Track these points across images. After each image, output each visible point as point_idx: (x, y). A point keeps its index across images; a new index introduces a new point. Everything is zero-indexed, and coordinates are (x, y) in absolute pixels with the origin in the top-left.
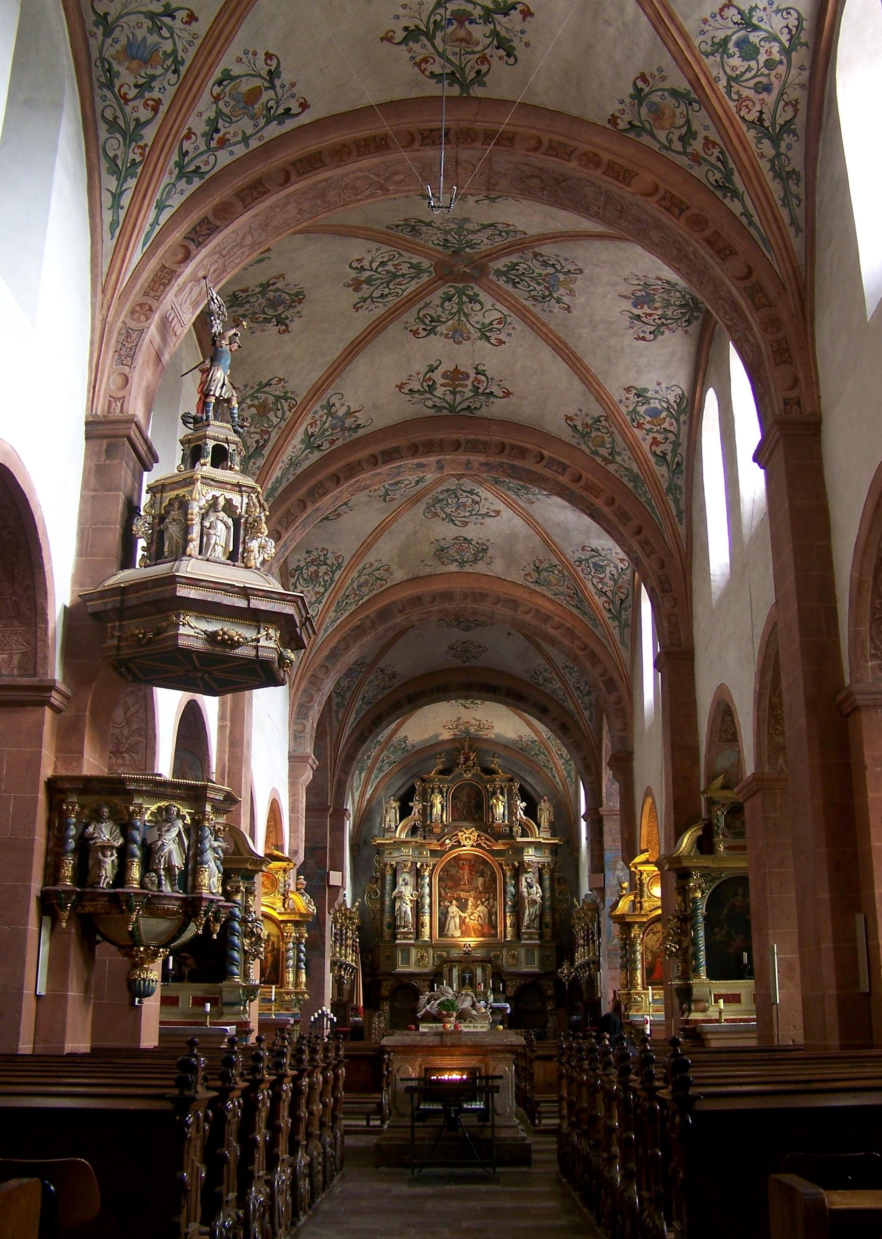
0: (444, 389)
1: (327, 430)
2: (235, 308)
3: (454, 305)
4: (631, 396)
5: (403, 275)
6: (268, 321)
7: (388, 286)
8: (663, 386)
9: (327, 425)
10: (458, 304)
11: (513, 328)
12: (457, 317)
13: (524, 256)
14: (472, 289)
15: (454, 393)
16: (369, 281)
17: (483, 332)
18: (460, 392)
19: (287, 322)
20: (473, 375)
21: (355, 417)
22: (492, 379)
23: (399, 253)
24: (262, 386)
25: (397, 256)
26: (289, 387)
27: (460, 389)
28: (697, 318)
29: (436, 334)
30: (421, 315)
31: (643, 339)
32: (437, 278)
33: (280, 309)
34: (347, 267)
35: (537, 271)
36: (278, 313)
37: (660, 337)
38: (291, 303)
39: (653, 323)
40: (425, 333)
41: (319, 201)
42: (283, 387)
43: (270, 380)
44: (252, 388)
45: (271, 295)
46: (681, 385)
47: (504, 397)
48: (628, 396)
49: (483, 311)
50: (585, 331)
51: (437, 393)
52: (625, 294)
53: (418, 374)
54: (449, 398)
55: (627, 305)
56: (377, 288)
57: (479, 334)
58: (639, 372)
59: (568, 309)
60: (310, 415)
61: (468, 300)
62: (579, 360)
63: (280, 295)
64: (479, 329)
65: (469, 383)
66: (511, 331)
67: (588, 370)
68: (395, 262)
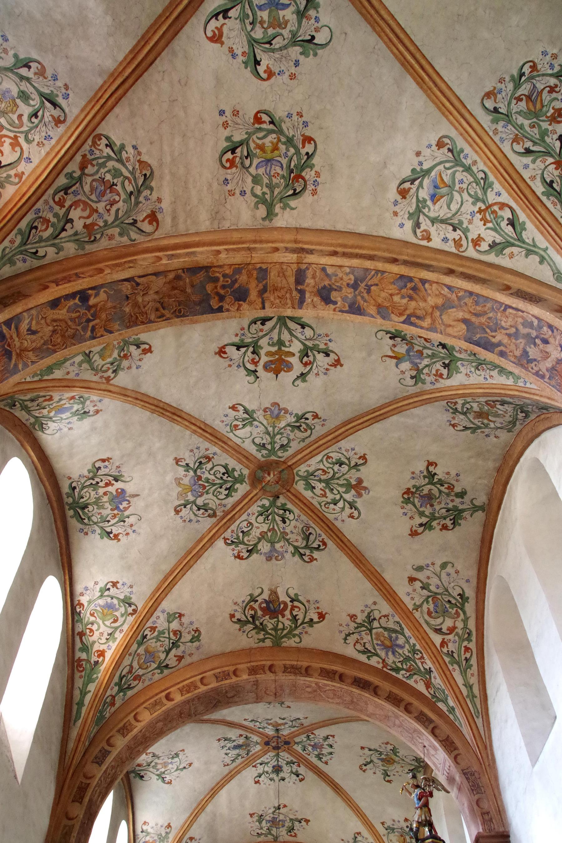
0: (291, 350)
1: (428, 356)
2: (461, 507)
3: (278, 441)
4: (92, 409)
5: (320, 481)
6: (441, 483)
7: (334, 474)
8: (65, 430)
9: (426, 362)
10: (275, 443)
11: (223, 422)
12: (276, 430)
13: (223, 508)
14: (262, 455)
15: (280, 343)
16: (349, 486)
17: (252, 417)
18: (273, 345)
19: (425, 473)
20: (260, 368)
21: (393, 351)
22: (239, 366)
23: (321, 506)
24: (474, 430)
25: (323, 504)
26: (448, 416)
27: (274, 349)
28: (68, 495)
29: (297, 415)
30: (309, 431)
31: (103, 461)
32: (293, 467)
33: (426, 491)
34: (362, 516)
35: (210, 496)
36: (429, 487)
37: (90, 467)
38: (415, 493)
39: (101, 477)
40: (307, 416)
41: (355, 700)
42: (454, 418)
43: (463, 430)
44: (483, 432)
45: (428, 511)
46: (49, 437)
47: (224, 347)
48: (96, 408)
49: (252, 437)
50: (158, 445)
51: (299, 346)
52: (136, 499)
53: (317, 374)
54: (286, 336)
55: (130, 488)
56: (344, 475)
57: (255, 415)
58: (93, 429)
59: (177, 461)
60: (438, 385)
61: (266, 446)
62: (153, 411)
63: (421, 506)
64: (255, 420)
65: (264, 359)
66: (225, 419)
67: (143, 407)
68: (324, 499)
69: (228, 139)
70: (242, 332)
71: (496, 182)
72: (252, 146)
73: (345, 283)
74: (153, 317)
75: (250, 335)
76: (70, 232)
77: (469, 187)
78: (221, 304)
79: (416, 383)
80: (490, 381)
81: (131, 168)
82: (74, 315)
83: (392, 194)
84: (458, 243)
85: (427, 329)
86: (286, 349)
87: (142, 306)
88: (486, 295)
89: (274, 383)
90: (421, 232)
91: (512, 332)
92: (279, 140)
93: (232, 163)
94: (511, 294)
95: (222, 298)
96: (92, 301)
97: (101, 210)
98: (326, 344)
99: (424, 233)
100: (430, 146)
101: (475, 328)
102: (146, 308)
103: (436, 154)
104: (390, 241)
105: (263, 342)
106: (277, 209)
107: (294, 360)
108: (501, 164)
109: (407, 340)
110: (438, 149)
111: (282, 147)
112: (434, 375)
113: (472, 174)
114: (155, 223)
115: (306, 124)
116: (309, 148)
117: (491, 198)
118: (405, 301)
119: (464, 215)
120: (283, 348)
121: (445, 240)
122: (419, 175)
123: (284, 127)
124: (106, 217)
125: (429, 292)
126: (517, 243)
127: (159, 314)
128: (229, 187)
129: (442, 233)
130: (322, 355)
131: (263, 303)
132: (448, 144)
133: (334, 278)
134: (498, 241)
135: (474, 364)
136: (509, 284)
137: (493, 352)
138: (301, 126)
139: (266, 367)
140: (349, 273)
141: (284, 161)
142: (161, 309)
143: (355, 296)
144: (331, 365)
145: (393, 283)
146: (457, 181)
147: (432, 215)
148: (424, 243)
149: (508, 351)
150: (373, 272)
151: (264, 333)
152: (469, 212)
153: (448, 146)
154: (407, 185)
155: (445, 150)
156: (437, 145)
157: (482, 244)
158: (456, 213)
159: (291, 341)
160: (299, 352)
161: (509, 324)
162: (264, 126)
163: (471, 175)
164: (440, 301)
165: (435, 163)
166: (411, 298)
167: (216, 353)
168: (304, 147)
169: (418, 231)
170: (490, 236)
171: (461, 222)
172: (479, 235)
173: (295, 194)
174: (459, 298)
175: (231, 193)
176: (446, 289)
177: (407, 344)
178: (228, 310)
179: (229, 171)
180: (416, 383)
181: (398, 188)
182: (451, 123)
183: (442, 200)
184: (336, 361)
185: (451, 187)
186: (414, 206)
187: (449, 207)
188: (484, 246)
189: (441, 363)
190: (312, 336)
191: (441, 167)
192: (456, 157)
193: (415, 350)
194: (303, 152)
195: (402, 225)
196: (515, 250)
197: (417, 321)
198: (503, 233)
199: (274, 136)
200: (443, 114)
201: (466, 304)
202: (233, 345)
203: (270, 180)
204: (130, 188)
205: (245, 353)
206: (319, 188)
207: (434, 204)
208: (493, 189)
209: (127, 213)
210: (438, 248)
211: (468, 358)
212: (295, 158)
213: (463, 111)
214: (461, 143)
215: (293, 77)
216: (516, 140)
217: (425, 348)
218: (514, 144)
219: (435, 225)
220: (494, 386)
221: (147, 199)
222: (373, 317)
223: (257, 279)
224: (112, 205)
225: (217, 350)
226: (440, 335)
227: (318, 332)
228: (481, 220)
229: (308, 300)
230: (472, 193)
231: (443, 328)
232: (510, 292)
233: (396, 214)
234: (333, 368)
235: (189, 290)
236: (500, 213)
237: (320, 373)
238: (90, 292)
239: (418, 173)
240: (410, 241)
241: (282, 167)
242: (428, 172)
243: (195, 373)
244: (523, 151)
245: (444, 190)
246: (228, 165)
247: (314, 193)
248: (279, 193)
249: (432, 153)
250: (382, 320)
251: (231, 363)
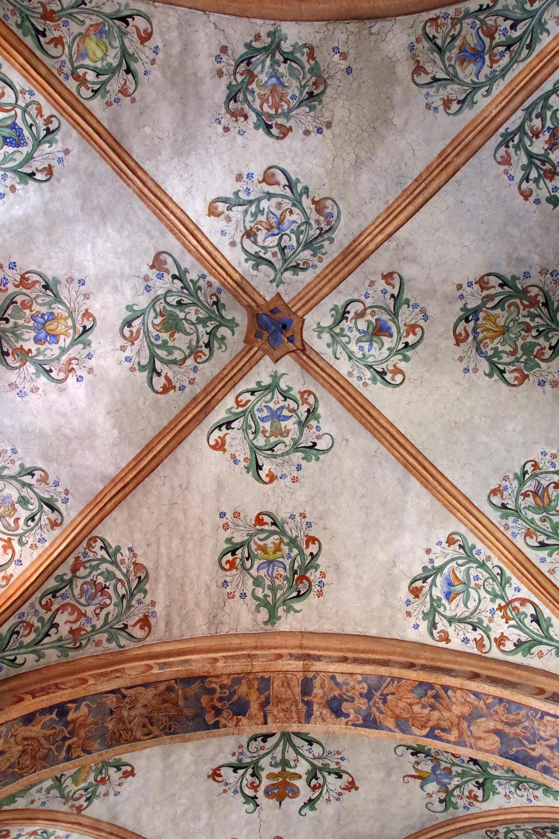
0: (296, 771)
1: (458, 775)
9: (456, 781)
15: (285, 763)
18: (276, 765)
21: (417, 770)
22: (235, 792)
47: (218, 768)
54: (291, 755)
60: (473, 810)
65: (265, 782)
69: (228, 540)
70: (240, 750)
71: (513, 577)
72: (253, 547)
73: (357, 693)
74: (138, 734)
75: (249, 754)
76: (54, 637)
77: (486, 583)
78: (217, 719)
79: (446, 809)
80: (535, 803)
81: (125, 571)
82: (49, 732)
83: (404, 593)
84: (479, 643)
85: (455, 743)
86: (292, 771)
87: (127, 722)
88: (518, 701)
89: (277, 811)
90: (438, 633)
91: (554, 743)
92: (281, 541)
93: (232, 565)
94: (547, 699)
95: (218, 712)
96: (71, 716)
97: (89, 614)
98: (337, 763)
99: (442, 634)
100: (439, 543)
101: (510, 740)
102: (132, 724)
103: (447, 551)
104: (404, 644)
105: (265, 762)
106: (280, 611)
107: (301, 784)
108: (516, 559)
109: (431, 756)
110: (449, 546)
111: (285, 549)
112: (467, 797)
113: (487, 570)
114: (147, 628)
115: (309, 525)
116: (313, 549)
117: (510, 594)
118: (426, 711)
119: (484, 613)
120: (288, 769)
121: (466, 640)
122: (430, 573)
123: (287, 528)
124: (94, 622)
125: (454, 700)
126: (544, 640)
127: (145, 730)
128: (228, 590)
129: (461, 633)
130: (333, 776)
131: (265, 717)
132: (458, 540)
133: (345, 687)
134: (523, 639)
135: (513, 783)
136: (542, 686)
137: (534, 768)
138: (304, 526)
139: (267, 793)
140: (362, 681)
141: (287, 562)
142: (149, 725)
143: (370, 707)
144: (344, 789)
145: (412, 691)
146: (472, 577)
147: (448, 613)
148: (442, 644)
149: (552, 766)
150: (388, 680)
151: (266, 751)
152: (488, 610)
153: (459, 543)
154: (419, 584)
155: (456, 546)
156: (447, 542)
157: (507, 643)
158: (475, 611)
159: (296, 760)
160: (306, 773)
161: (548, 733)
162: (266, 527)
163: (486, 571)
164: (466, 710)
165: (446, 560)
166: (433, 708)
167: (209, 777)
168: (307, 547)
169: (435, 632)
170: (514, 635)
171: (481, 621)
172: (502, 633)
173: (299, 596)
174: (488, 706)
175: (231, 596)
176: (472, 696)
177: (432, 761)
178: (225, 726)
179: (229, 573)
180: (446, 809)
181: (409, 587)
182: (460, 520)
183: (458, 598)
184: (349, 783)
185: (466, 584)
186: (428, 605)
187: (466, 605)
188: (509, 646)
189: (474, 782)
190: (321, 753)
191: (454, 564)
192: (469, 554)
193: (442, 767)
194: (307, 552)
195: (416, 627)
196: (544, 648)
197: (442, 734)
198: (527, 631)
199: (276, 537)
200: (451, 511)
201: (496, 712)
202: (229, 766)
203: (273, 582)
204: (122, 591)
205: (243, 775)
206: (325, 589)
207: (450, 602)
208: (511, 584)
209: (118, 617)
210: (459, 649)
211: (506, 775)
212: (298, 558)
213: (470, 508)
214: (472, 539)
215: (295, 480)
216: (528, 534)
217: (454, 764)
218: (528, 538)
219: (453, 625)
220: (540, 809)
221: (139, 602)
222: (390, 730)
223: (258, 689)
224: (102, 609)
225: (211, 772)
226: (470, 750)
227: (328, 749)
228: (502, 617)
229: (317, 713)
230: (490, 590)
231: (472, 741)
232: (546, 696)
233: (409, 614)
234: (346, 792)
235: (181, 703)
236: (522, 609)
237: (331, 798)
238: (70, 705)
239: (430, 570)
240: (427, 643)
241: (285, 568)
242: (440, 569)
243: (183, 801)
244: (538, 545)
245: (460, 588)
246: (227, 567)
247: (320, 594)
248: (282, 595)
249: (443, 550)
250: (402, 734)
251: (226, 788)
